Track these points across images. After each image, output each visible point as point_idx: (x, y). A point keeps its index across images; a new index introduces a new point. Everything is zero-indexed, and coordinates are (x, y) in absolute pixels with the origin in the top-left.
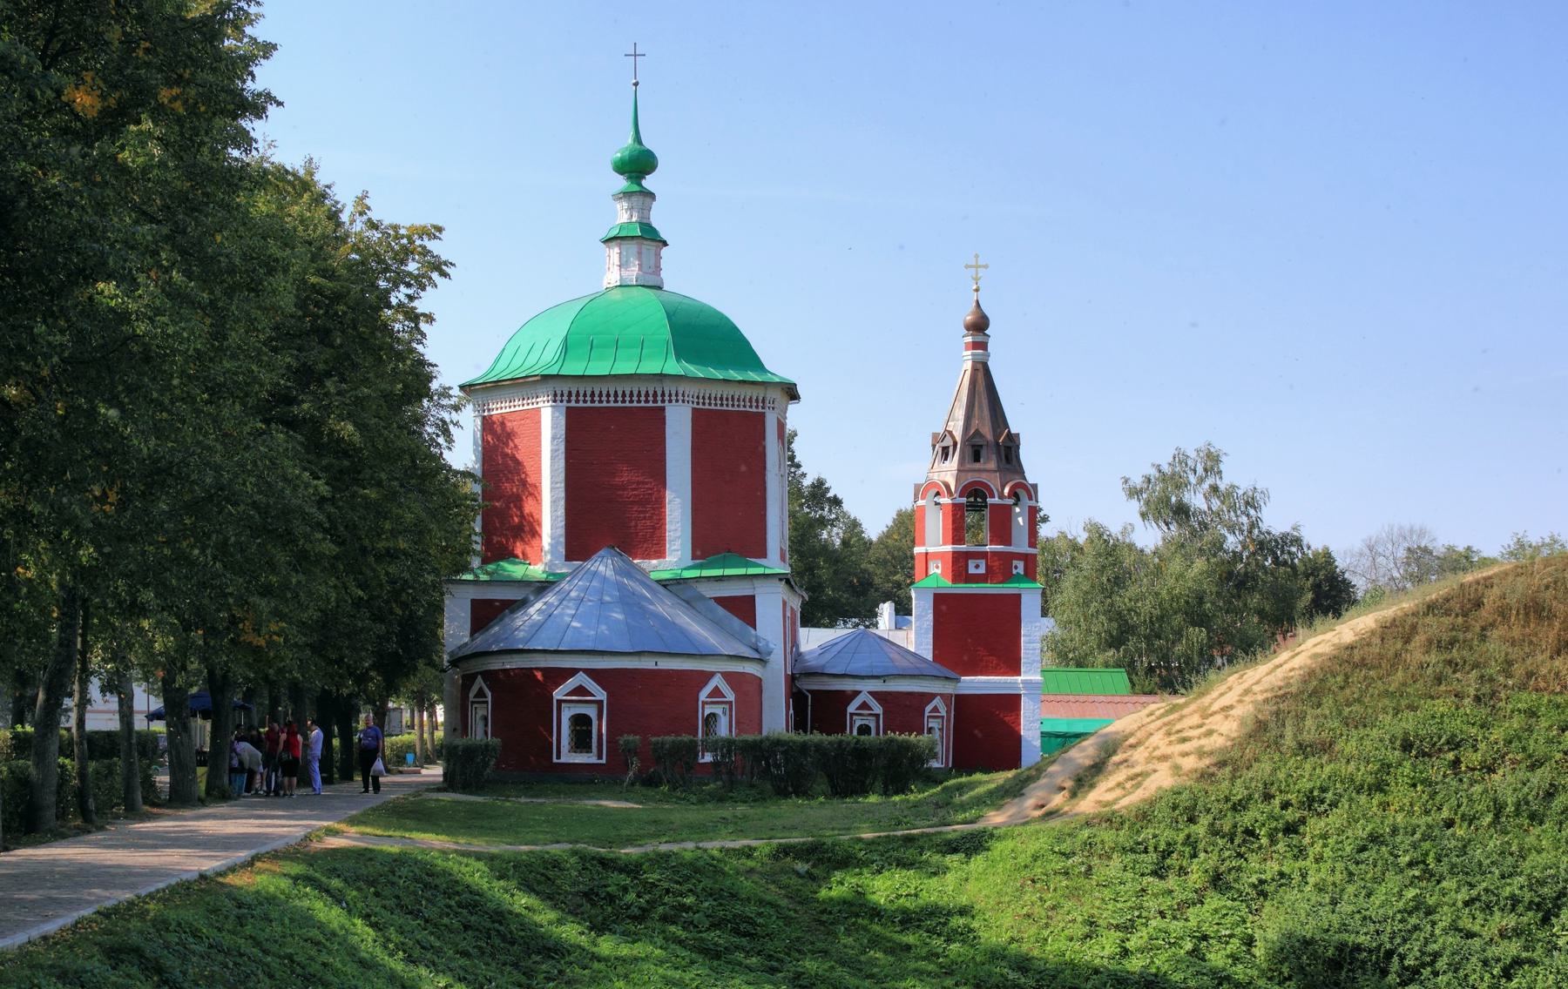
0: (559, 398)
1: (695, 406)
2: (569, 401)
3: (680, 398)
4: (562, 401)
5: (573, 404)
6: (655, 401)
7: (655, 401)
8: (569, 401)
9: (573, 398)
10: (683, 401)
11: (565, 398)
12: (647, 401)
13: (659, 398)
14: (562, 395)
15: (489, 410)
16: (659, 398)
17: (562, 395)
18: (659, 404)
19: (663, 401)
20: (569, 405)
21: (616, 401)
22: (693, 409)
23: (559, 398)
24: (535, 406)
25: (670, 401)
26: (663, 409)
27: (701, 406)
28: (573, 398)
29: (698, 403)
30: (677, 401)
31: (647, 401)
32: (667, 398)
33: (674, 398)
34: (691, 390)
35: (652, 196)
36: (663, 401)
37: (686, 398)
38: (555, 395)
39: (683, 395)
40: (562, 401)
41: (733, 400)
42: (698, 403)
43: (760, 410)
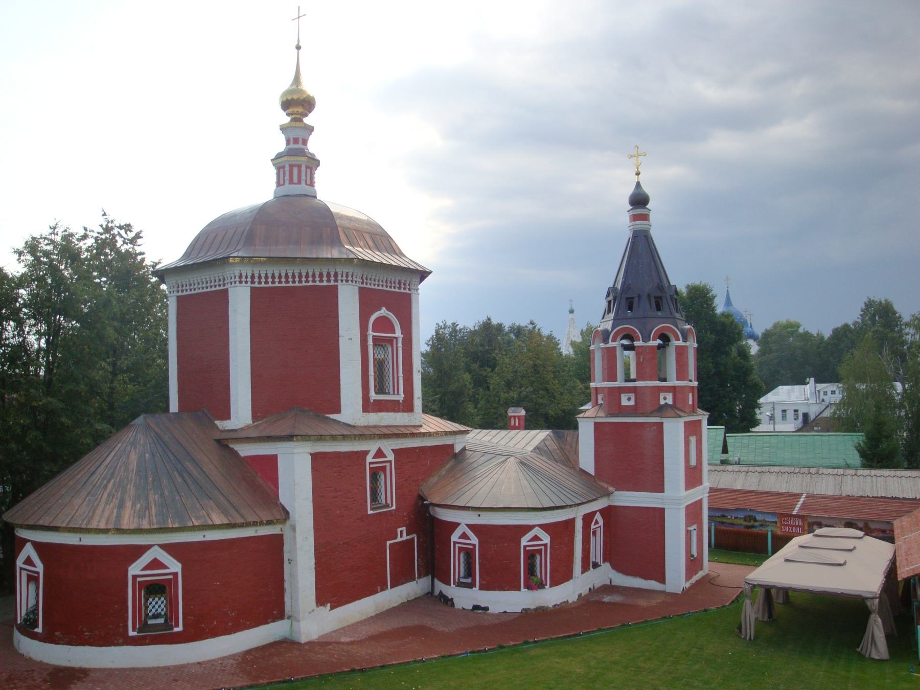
0: (244, 279)
2: (253, 282)
3: (350, 278)
4: (246, 282)
5: (256, 285)
6: (329, 281)
7: (329, 281)
8: (253, 282)
9: (256, 280)
10: (352, 281)
11: (249, 279)
13: (332, 278)
14: (246, 277)
15: (182, 291)
16: (332, 278)
17: (246, 277)
18: (332, 283)
19: (336, 281)
21: (294, 282)
22: (361, 290)
24: (222, 288)
25: (342, 281)
26: (336, 287)
27: (364, 285)
28: (256, 280)
30: (347, 281)
31: (321, 281)
32: (339, 278)
34: (358, 272)
35: (310, 129)
36: (336, 281)
37: (355, 279)
38: (241, 277)
39: (352, 276)
40: (246, 282)
41: (387, 282)
42: (362, 283)
43: (407, 291)
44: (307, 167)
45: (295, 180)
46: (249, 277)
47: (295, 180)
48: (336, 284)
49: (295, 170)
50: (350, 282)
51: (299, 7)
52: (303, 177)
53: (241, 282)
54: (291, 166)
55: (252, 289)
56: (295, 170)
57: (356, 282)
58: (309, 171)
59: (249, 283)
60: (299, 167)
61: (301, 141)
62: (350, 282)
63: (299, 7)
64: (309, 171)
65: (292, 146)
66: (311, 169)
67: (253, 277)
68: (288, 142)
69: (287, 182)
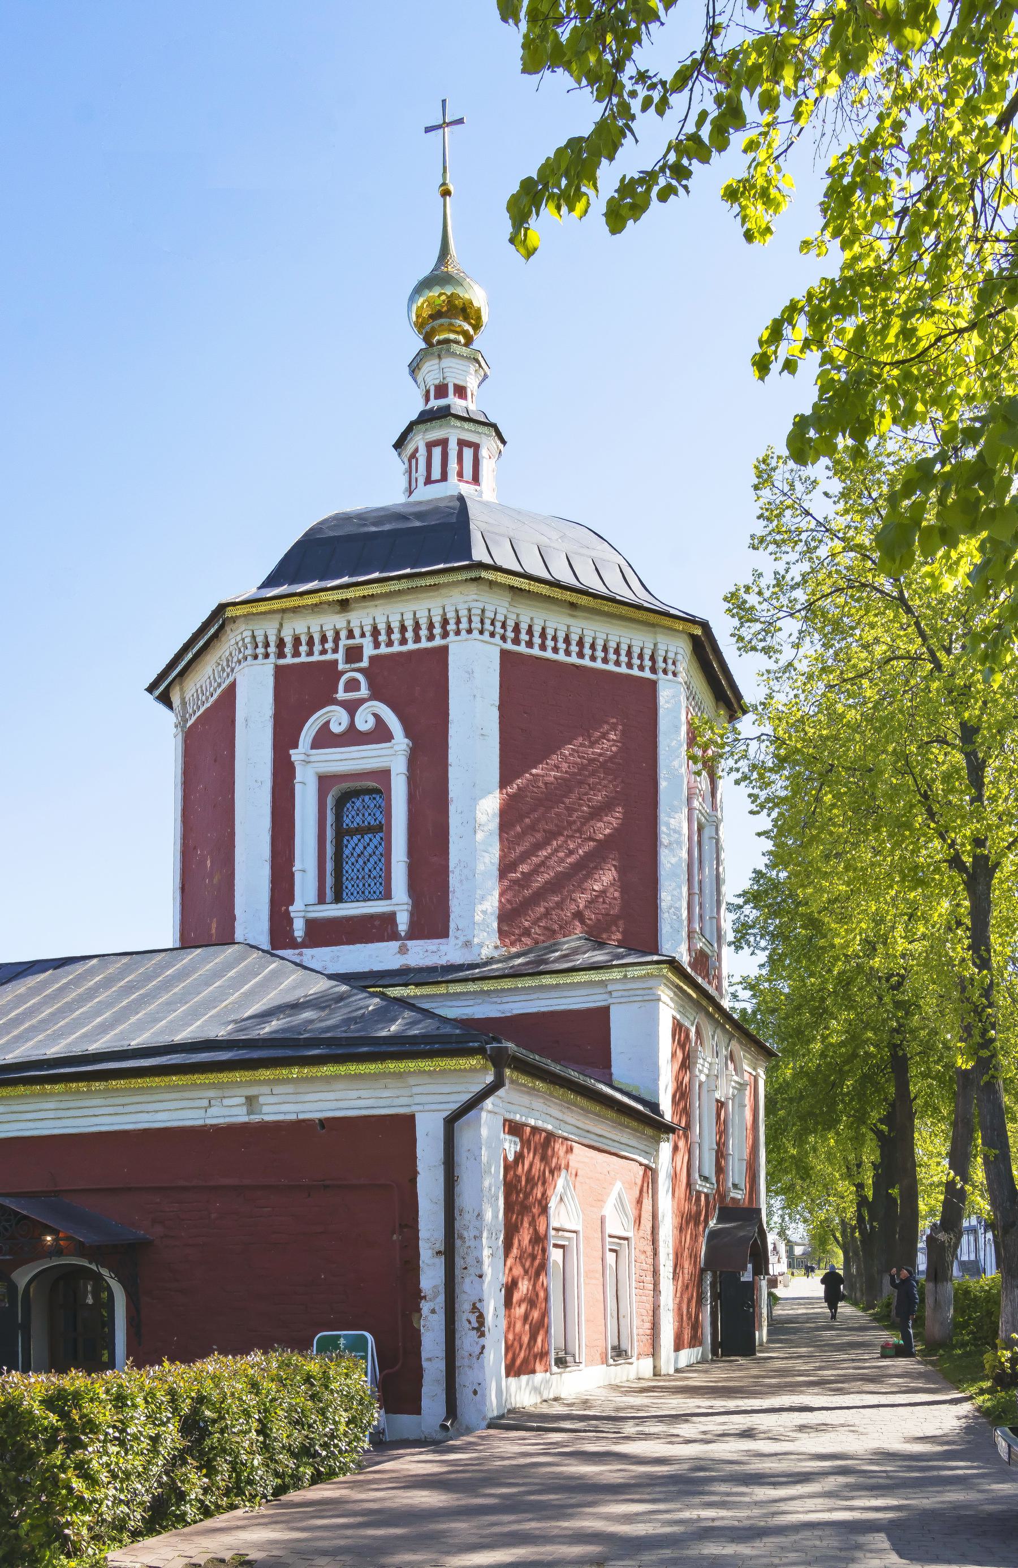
1: (509, 646)
2: (281, 655)
3: (476, 624)
5: (289, 660)
8: (281, 655)
11: (272, 649)
12: (417, 639)
13: (437, 631)
14: (267, 645)
16: (437, 631)
17: (267, 645)
18: (438, 642)
19: (445, 635)
20: (282, 662)
23: (260, 650)
25: (458, 633)
26: (444, 650)
29: (516, 641)
30: (469, 631)
31: (417, 639)
32: (451, 627)
33: (464, 625)
36: (445, 635)
37: (488, 626)
40: (267, 656)
44: (462, 443)
45: (436, 474)
46: (272, 644)
47: (436, 474)
48: (443, 642)
49: (437, 452)
50: (476, 633)
51: (444, 101)
52: (453, 466)
53: (256, 657)
54: (430, 446)
55: (279, 670)
56: (437, 452)
57: (492, 635)
58: (468, 453)
59: (272, 658)
60: (444, 443)
61: (451, 390)
62: (476, 633)
63: (444, 101)
64: (468, 453)
65: (435, 403)
66: (476, 447)
67: (281, 644)
68: (427, 400)
69: (421, 480)
